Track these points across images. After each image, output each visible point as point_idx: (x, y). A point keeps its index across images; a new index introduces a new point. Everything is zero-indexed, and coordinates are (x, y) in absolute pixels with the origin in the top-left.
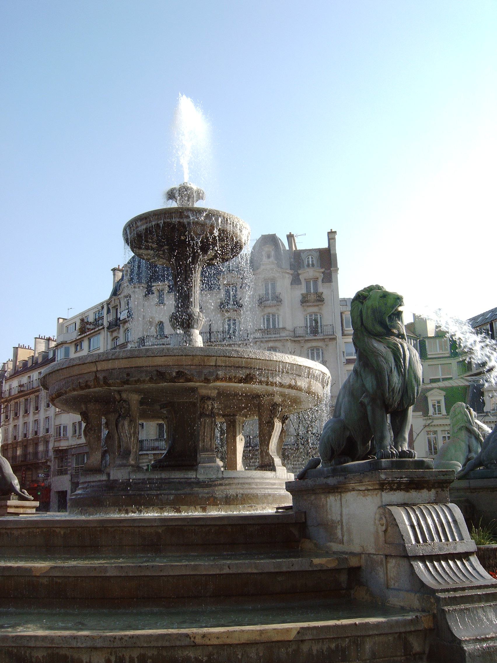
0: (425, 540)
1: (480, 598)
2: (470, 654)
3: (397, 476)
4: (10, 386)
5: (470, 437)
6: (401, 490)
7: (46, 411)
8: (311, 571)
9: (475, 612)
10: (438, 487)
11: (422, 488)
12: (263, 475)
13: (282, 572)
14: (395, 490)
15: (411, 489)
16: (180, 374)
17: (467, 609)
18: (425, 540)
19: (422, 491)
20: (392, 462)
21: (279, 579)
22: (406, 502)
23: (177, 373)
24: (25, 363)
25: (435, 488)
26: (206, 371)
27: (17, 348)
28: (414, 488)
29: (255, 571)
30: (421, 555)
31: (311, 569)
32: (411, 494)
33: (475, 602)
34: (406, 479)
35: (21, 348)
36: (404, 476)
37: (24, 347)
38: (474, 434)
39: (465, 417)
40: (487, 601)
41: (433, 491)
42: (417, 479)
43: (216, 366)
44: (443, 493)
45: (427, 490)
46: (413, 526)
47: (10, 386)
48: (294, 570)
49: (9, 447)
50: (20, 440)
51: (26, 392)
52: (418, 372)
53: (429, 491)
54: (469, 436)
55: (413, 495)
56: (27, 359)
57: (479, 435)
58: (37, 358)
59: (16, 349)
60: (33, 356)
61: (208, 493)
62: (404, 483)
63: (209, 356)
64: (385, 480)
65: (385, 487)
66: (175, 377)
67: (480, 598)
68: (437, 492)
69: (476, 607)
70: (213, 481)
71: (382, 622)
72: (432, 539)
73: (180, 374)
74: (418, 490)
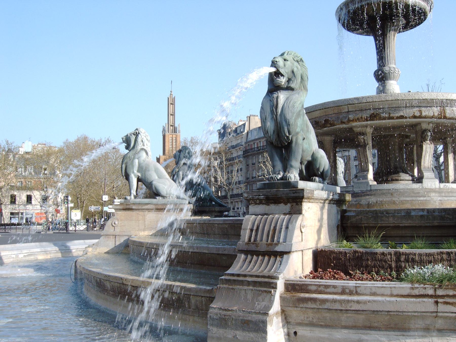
0: (255, 240)
1: (249, 283)
2: (210, 317)
3: (255, 194)
6: (263, 204)
8: (234, 255)
9: (238, 292)
10: (293, 202)
11: (280, 203)
12: (407, 187)
13: (224, 254)
14: (259, 204)
15: (271, 203)
16: (326, 121)
17: (233, 289)
18: (255, 240)
19: (280, 205)
20: (264, 184)
21: (224, 258)
22: (266, 213)
23: (325, 121)
25: (290, 203)
26: (341, 117)
28: (273, 203)
29: (207, 252)
30: (246, 250)
31: (234, 254)
32: (270, 207)
33: (245, 286)
34: (263, 196)
36: (261, 195)
40: (254, 286)
41: (289, 205)
42: (271, 196)
43: (348, 112)
44: (297, 206)
45: (284, 204)
46: (252, 230)
48: (225, 253)
52: (288, 115)
53: (285, 205)
55: (273, 207)
61: (356, 201)
62: (263, 199)
63: (339, 106)
64: (247, 197)
65: (250, 202)
66: (324, 124)
67: (249, 283)
68: (292, 205)
69: (241, 289)
70: (364, 193)
71: (194, 288)
72: (261, 240)
73: (326, 121)
74: (276, 204)
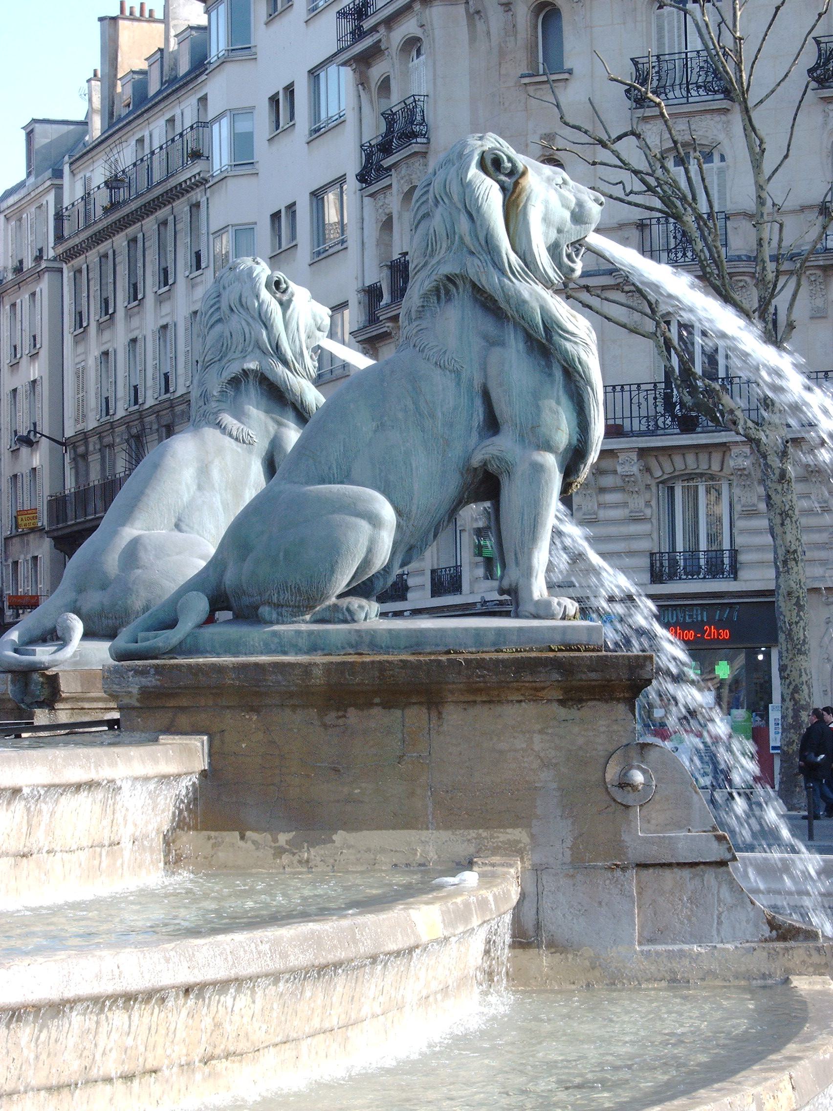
4: (87, 182)
5: (493, 342)
7: (192, 283)
24: (140, 79)
27: (114, 19)
35: (132, 18)
37: (144, 16)
38: (516, 325)
39: (464, 220)
47: (87, 182)
49: (91, 448)
50: (121, 413)
51: (133, 206)
54: (486, 338)
56: (144, 66)
57: (551, 326)
58: (175, 56)
59: (110, 24)
60: (161, 50)
